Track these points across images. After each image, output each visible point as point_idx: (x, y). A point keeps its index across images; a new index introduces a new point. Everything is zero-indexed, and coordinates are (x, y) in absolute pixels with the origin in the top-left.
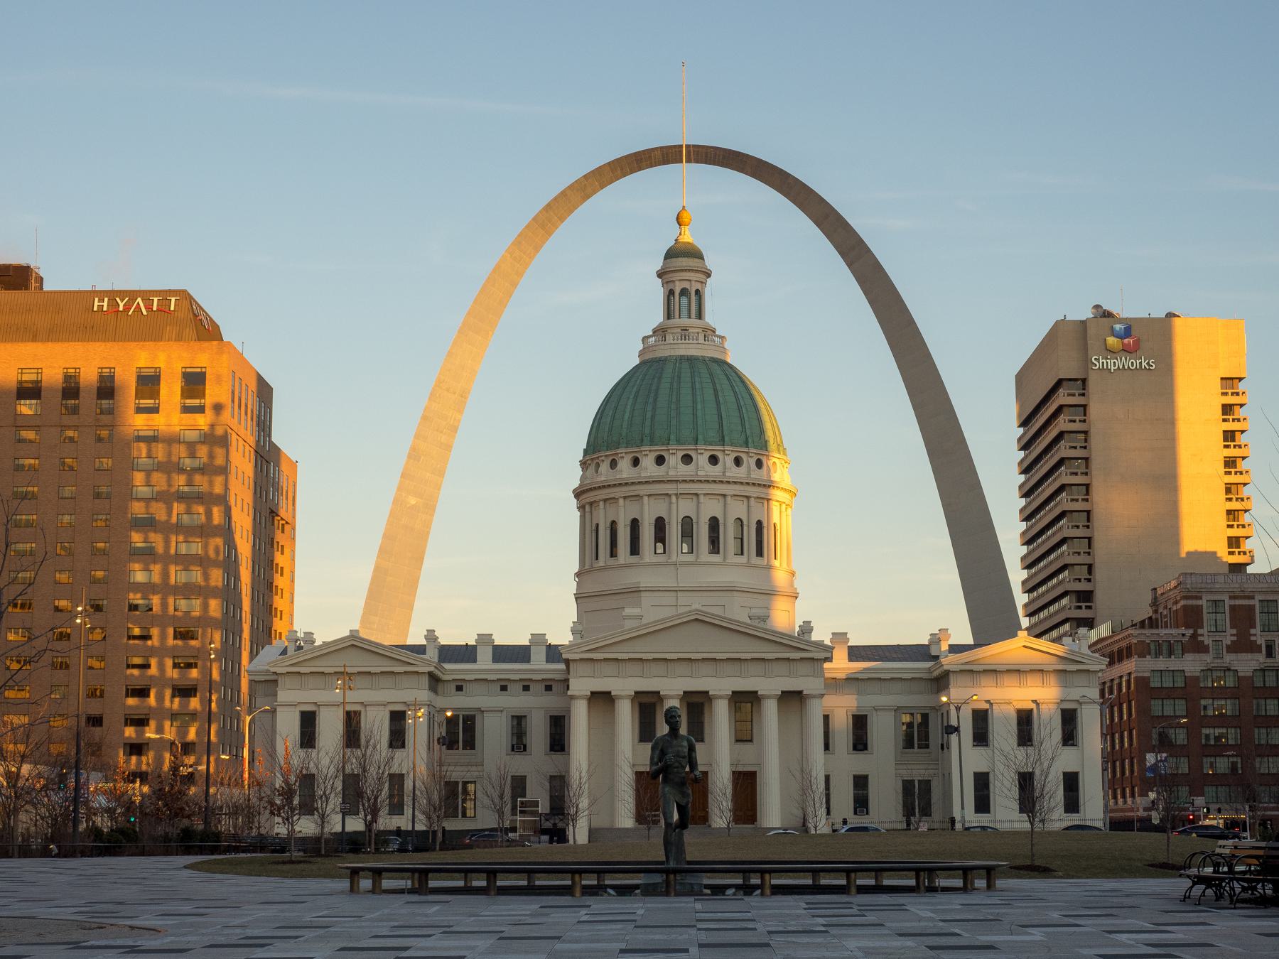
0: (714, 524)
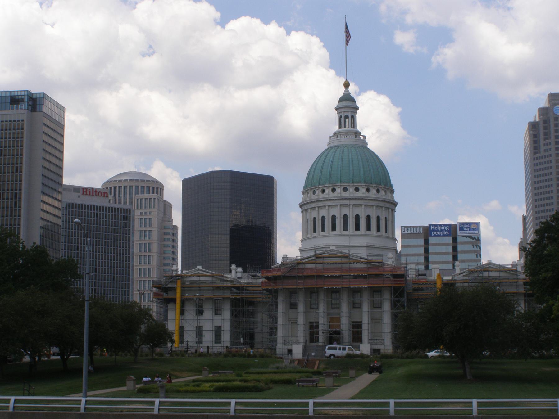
0: (357, 218)
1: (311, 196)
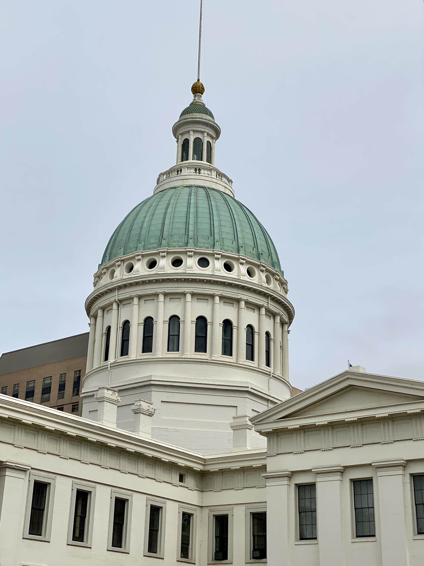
0: (227, 325)
1: (121, 274)
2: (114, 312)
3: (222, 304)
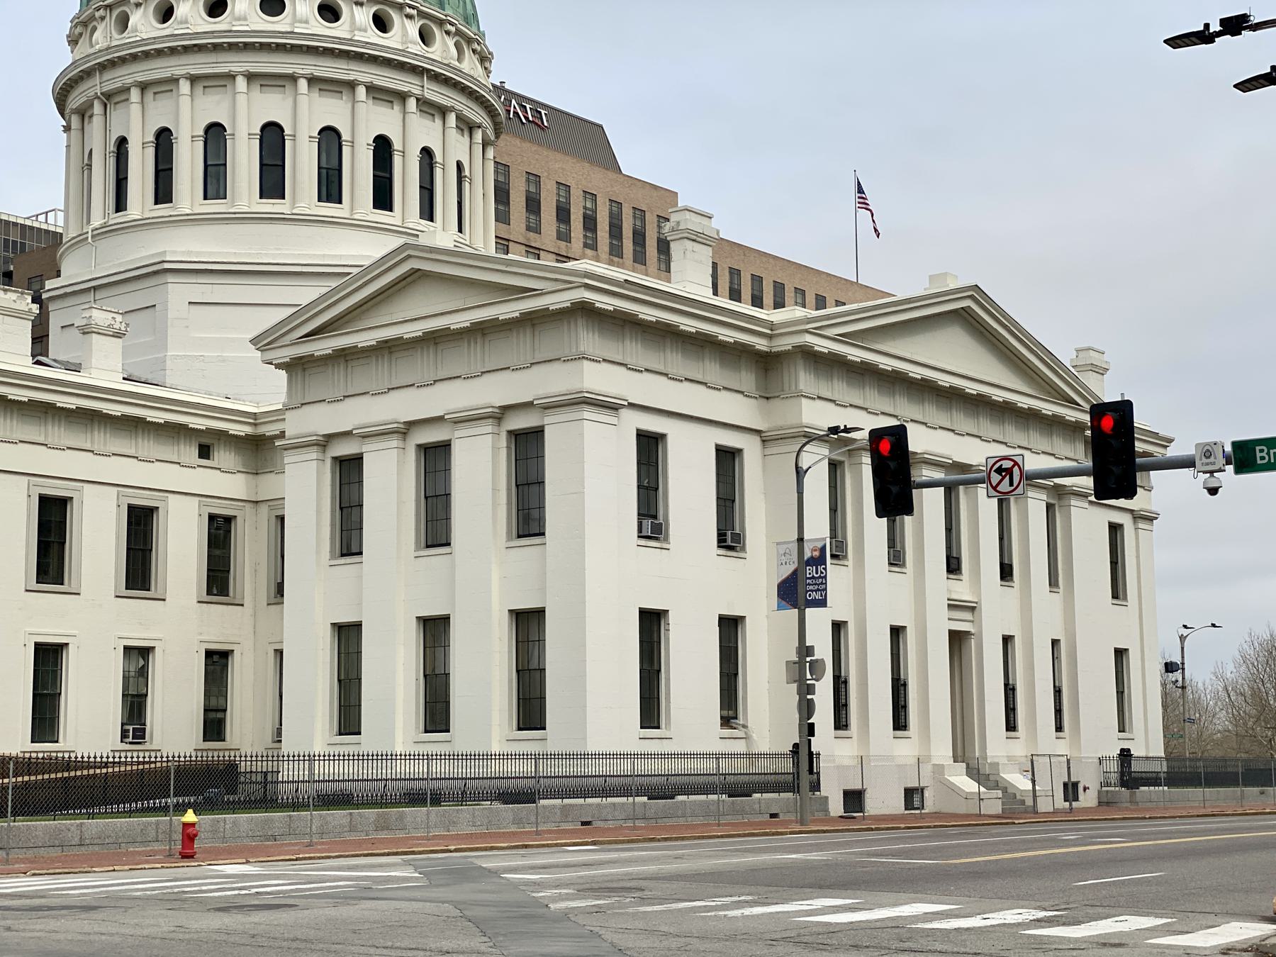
0: (330, 138)
1: (104, 37)
2: (97, 121)
3: (315, 94)
